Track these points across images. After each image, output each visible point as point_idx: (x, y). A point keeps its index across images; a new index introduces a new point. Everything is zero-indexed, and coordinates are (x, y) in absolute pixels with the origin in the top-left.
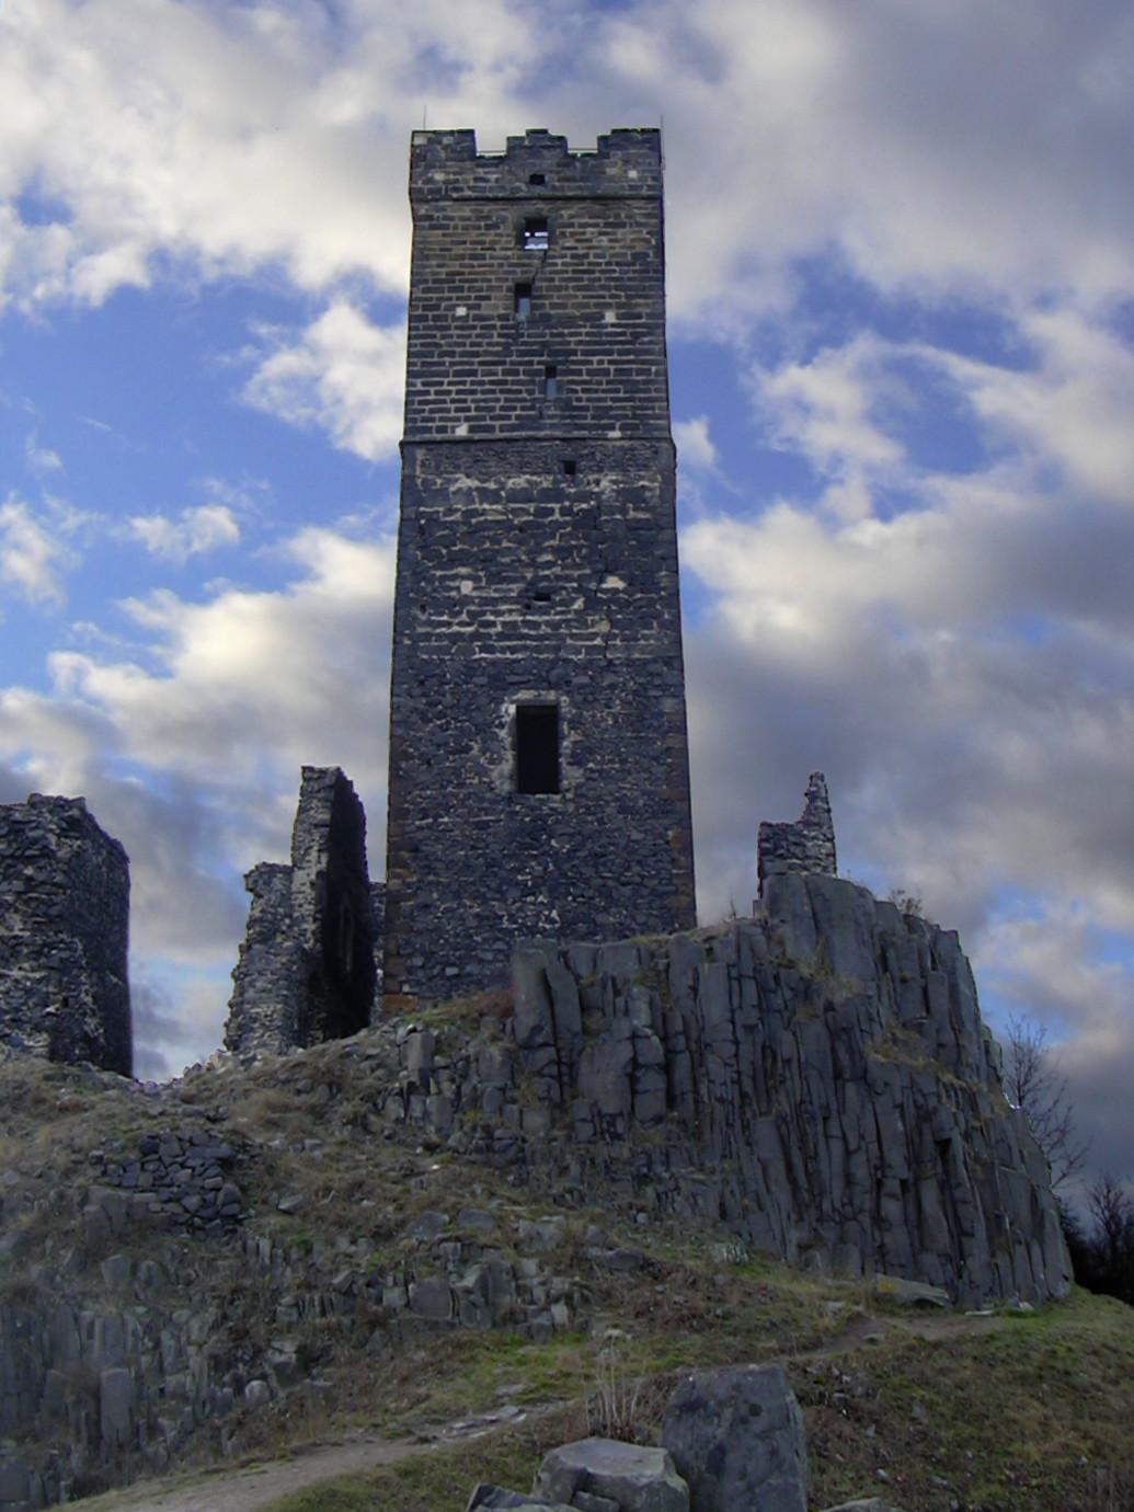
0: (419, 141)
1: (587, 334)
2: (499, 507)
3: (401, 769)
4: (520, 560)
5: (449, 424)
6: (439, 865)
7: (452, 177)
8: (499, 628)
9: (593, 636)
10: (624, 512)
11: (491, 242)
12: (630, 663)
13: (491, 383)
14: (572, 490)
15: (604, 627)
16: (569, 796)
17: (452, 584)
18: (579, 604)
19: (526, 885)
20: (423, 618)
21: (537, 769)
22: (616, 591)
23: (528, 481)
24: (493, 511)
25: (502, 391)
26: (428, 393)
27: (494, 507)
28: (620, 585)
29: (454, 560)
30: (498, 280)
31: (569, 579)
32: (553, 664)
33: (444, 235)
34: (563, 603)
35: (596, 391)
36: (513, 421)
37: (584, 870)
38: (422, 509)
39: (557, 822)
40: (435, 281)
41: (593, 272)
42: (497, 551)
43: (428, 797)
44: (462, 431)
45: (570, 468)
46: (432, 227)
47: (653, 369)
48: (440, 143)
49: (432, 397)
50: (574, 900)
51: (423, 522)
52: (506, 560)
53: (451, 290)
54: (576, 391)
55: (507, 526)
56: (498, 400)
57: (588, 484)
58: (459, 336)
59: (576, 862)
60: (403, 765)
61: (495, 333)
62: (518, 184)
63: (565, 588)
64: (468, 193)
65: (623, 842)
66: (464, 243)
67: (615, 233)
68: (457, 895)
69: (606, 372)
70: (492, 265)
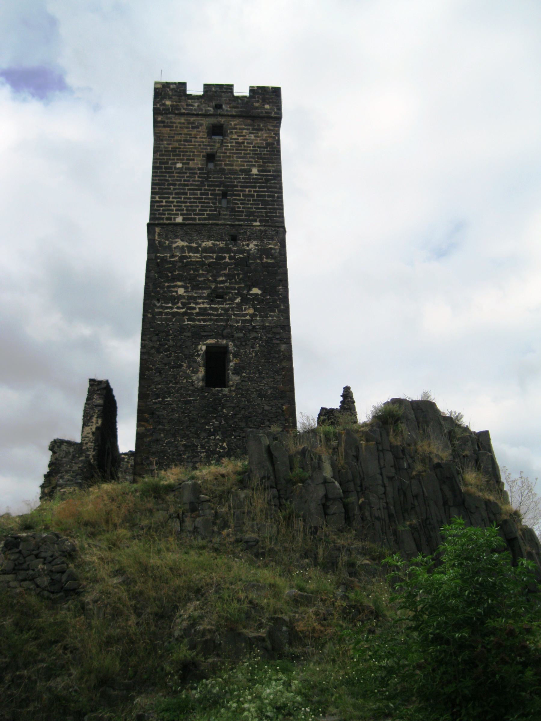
0: (159, 86)
1: (243, 178)
2: (198, 255)
3: (145, 375)
4: (208, 280)
5: (173, 216)
6: (164, 421)
7: (175, 103)
8: (197, 310)
9: (247, 314)
10: (261, 258)
11: (194, 134)
12: (264, 327)
13: (194, 198)
14: (235, 248)
15: (251, 311)
16: (233, 389)
17: (173, 289)
18: (238, 300)
19: (210, 431)
20: (158, 305)
21: (216, 373)
22: (257, 295)
23: (212, 244)
24: (195, 257)
25: (200, 203)
26: (162, 202)
27: (196, 255)
28: (259, 292)
29: (175, 279)
30: (198, 151)
31: (235, 289)
32: (225, 327)
33: (170, 130)
34: (230, 299)
35: (248, 204)
36: (205, 216)
37: (240, 424)
38: (158, 255)
39: (227, 401)
40: (166, 151)
41: (246, 150)
42: (197, 275)
43: (160, 388)
44: (179, 220)
45: (234, 239)
46: (164, 127)
47: (276, 195)
48: (169, 87)
49: (164, 204)
50: (235, 438)
51: (159, 261)
52: (201, 279)
53: (174, 155)
54: (238, 204)
56: (198, 206)
57: (243, 245)
58: (177, 177)
59: (236, 420)
60: (147, 373)
61: (197, 176)
62: (209, 108)
63: (232, 293)
64: (183, 111)
65: (260, 412)
66: (181, 134)
67: (258, 133)
68: (174, 436)
69: (253, 196)
70: (195, 145)
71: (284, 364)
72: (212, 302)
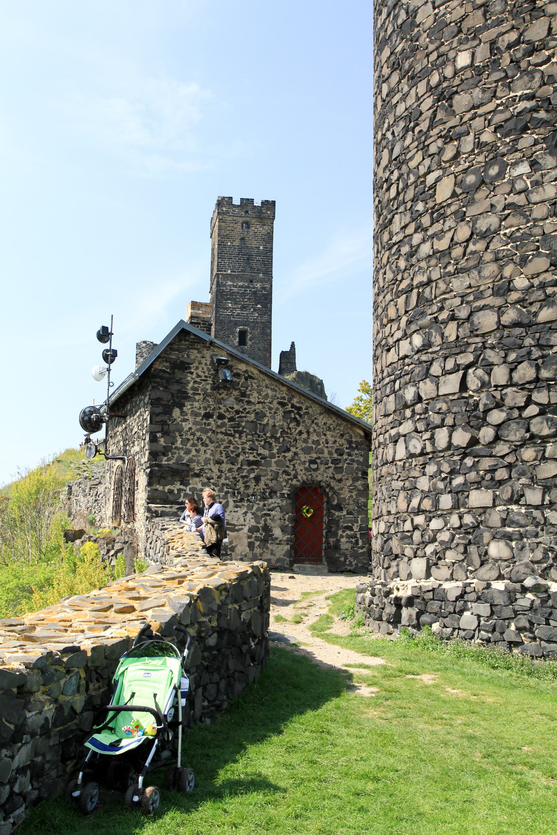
12: (261, 322)
24: (235, 290)
44: (229, 272)
45: (251, 281)
55: (238, 293)
71: (269, 338)
72: (242, 310)
